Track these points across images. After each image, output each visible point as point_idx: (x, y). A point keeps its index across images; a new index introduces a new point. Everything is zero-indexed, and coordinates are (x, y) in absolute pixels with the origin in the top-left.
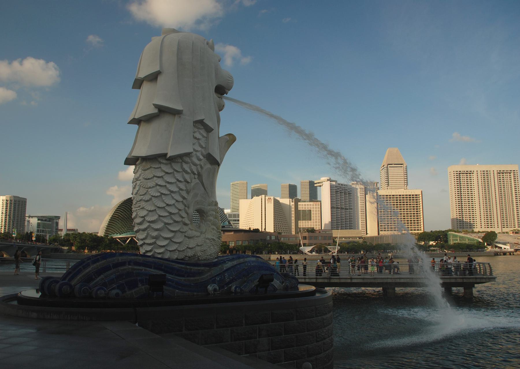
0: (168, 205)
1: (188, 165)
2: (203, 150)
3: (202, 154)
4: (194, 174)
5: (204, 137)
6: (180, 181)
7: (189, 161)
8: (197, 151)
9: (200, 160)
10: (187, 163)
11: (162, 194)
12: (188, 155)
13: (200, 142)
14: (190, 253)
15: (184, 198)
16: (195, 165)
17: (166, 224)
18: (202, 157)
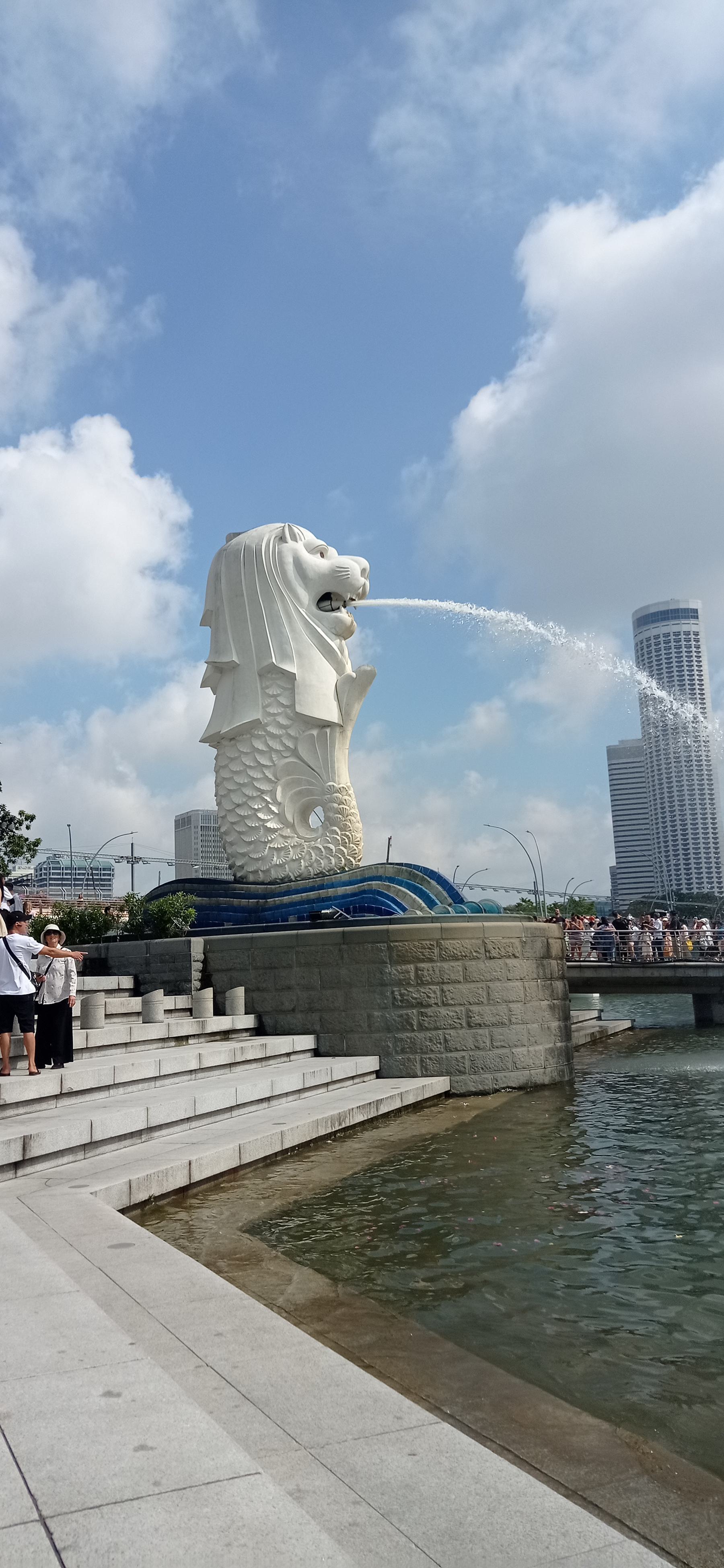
0: (238, 806)
1: (263, 739)
2: (289, 711)
3: (288, 718)
4: (277, 751)
5: (284, 689)
6: (250, 767)
7: (263, 733)
8: (274, 715)
9: (281, 726)
10: (259, 737)
11: (230, 790)
12: (256, 724)
13: (278, 698)
14: (281, 874)
15: (263, 792)
16: (273, 736)
17: (240, 833)
18: (283, 721)
